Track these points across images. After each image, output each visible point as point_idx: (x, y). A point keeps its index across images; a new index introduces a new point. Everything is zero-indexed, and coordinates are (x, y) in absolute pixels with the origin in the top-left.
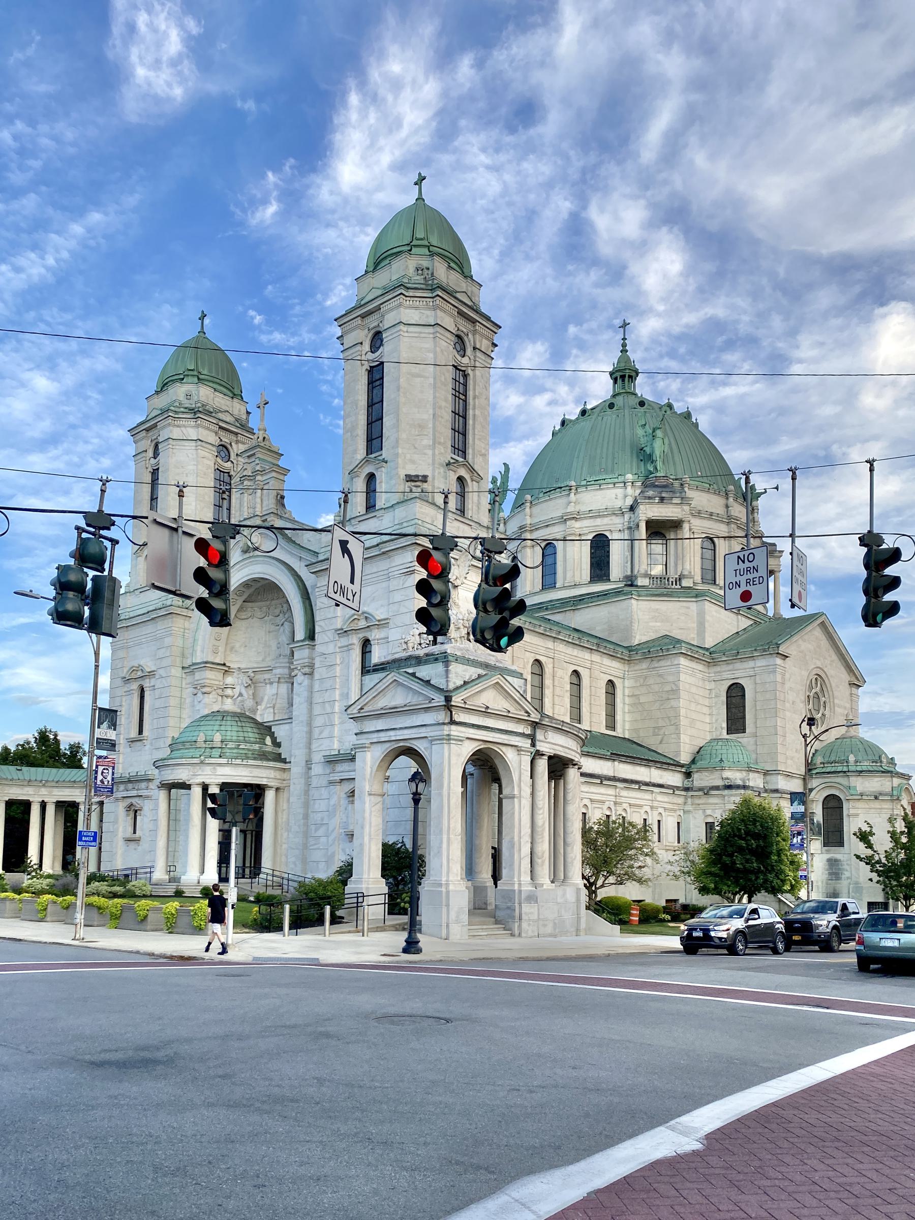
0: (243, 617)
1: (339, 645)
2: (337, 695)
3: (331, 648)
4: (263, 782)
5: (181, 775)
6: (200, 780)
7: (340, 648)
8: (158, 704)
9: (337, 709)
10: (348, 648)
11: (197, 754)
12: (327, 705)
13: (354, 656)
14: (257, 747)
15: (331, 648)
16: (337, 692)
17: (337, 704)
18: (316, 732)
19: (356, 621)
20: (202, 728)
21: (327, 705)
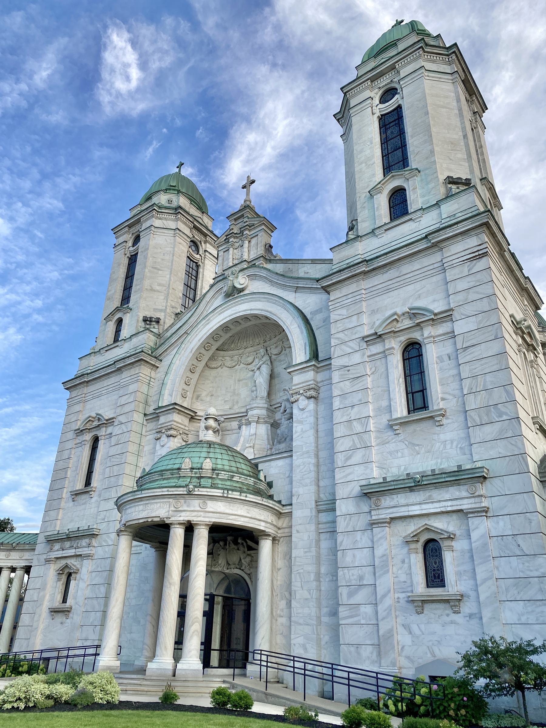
0: (213, 366)
1: (369, 354)
2: (370, 410)
3: (357, 358)
4: (262, 526)
5: (157, 511)
6: (184, 517)
7: (369, 356)
8: (113, 451)
9: (372, 426)
10: (385, 354)
11: (181, 482)
12: (355, 423)
13: (395, 362)
14: (251, 481)
15: (357, 358)
16: (371, 407)
17: (371, 421)
18: (340, 459)
19: (395, 323)
20: (186, 455)
21: (355, 423)
